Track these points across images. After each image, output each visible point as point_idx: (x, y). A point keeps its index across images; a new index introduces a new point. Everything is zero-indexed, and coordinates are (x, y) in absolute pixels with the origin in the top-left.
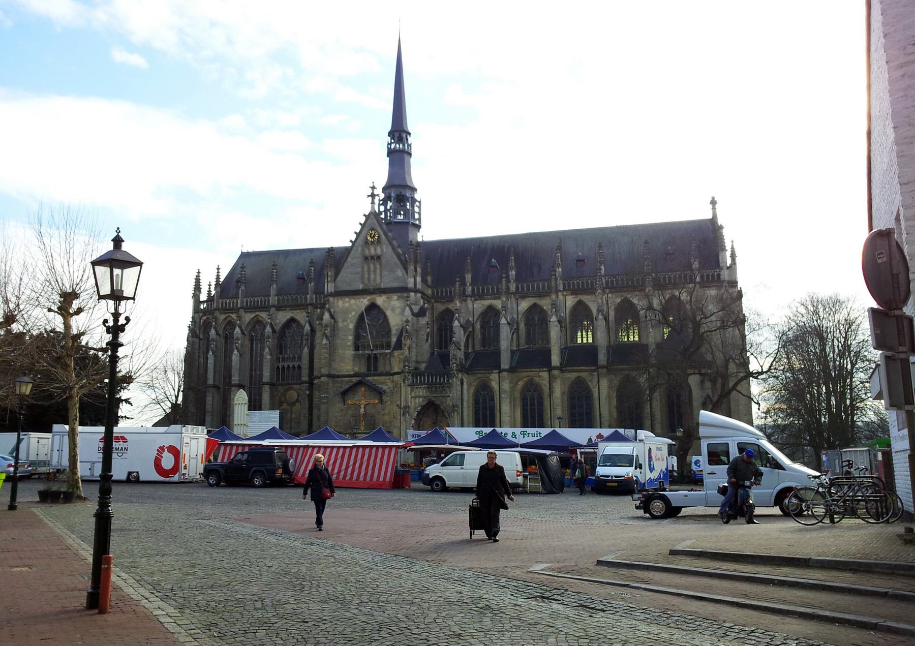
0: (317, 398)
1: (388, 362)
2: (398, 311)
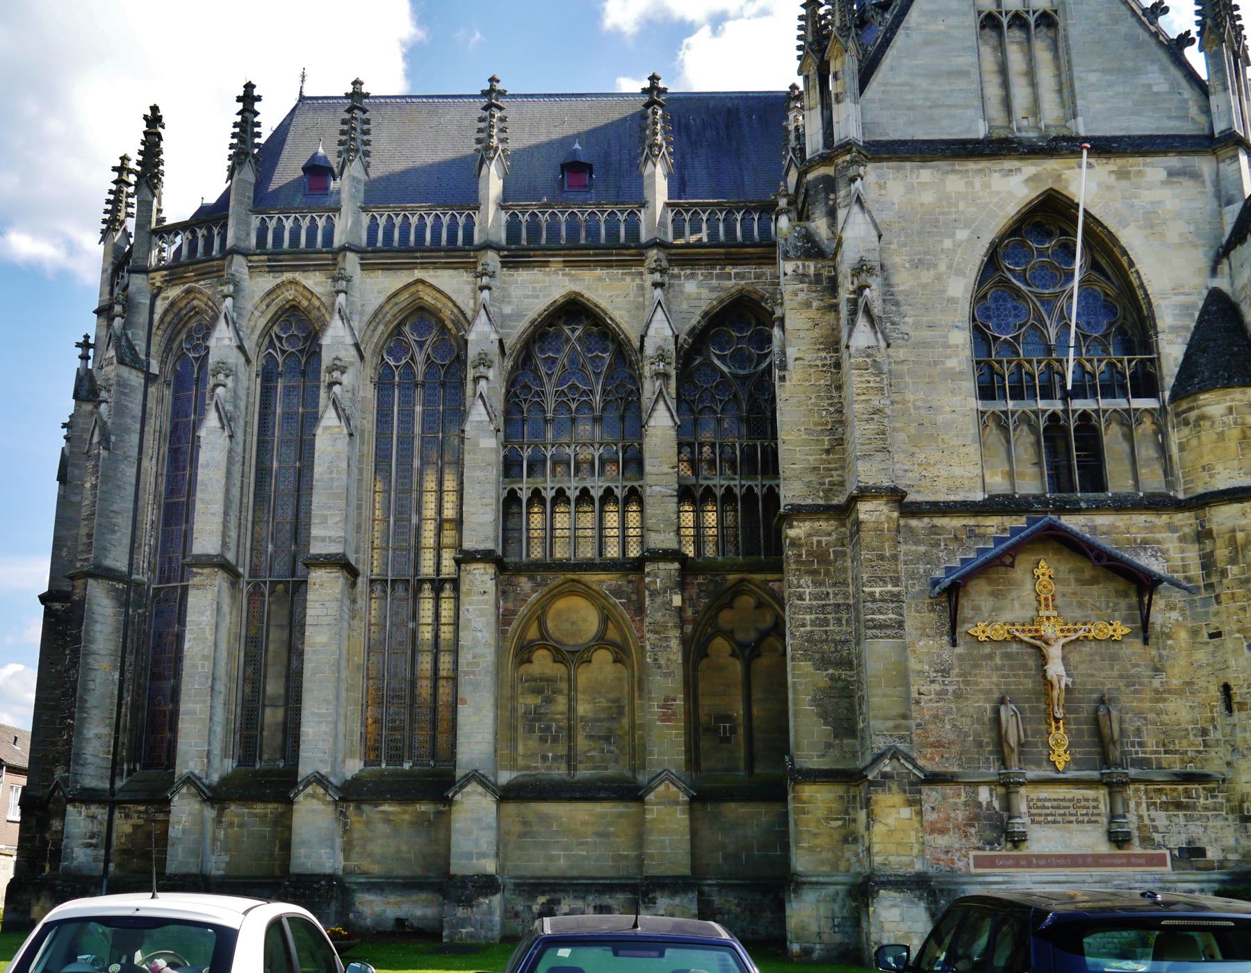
0: (810, 609)
1: (1147, 452)
2: (1175, 231)
